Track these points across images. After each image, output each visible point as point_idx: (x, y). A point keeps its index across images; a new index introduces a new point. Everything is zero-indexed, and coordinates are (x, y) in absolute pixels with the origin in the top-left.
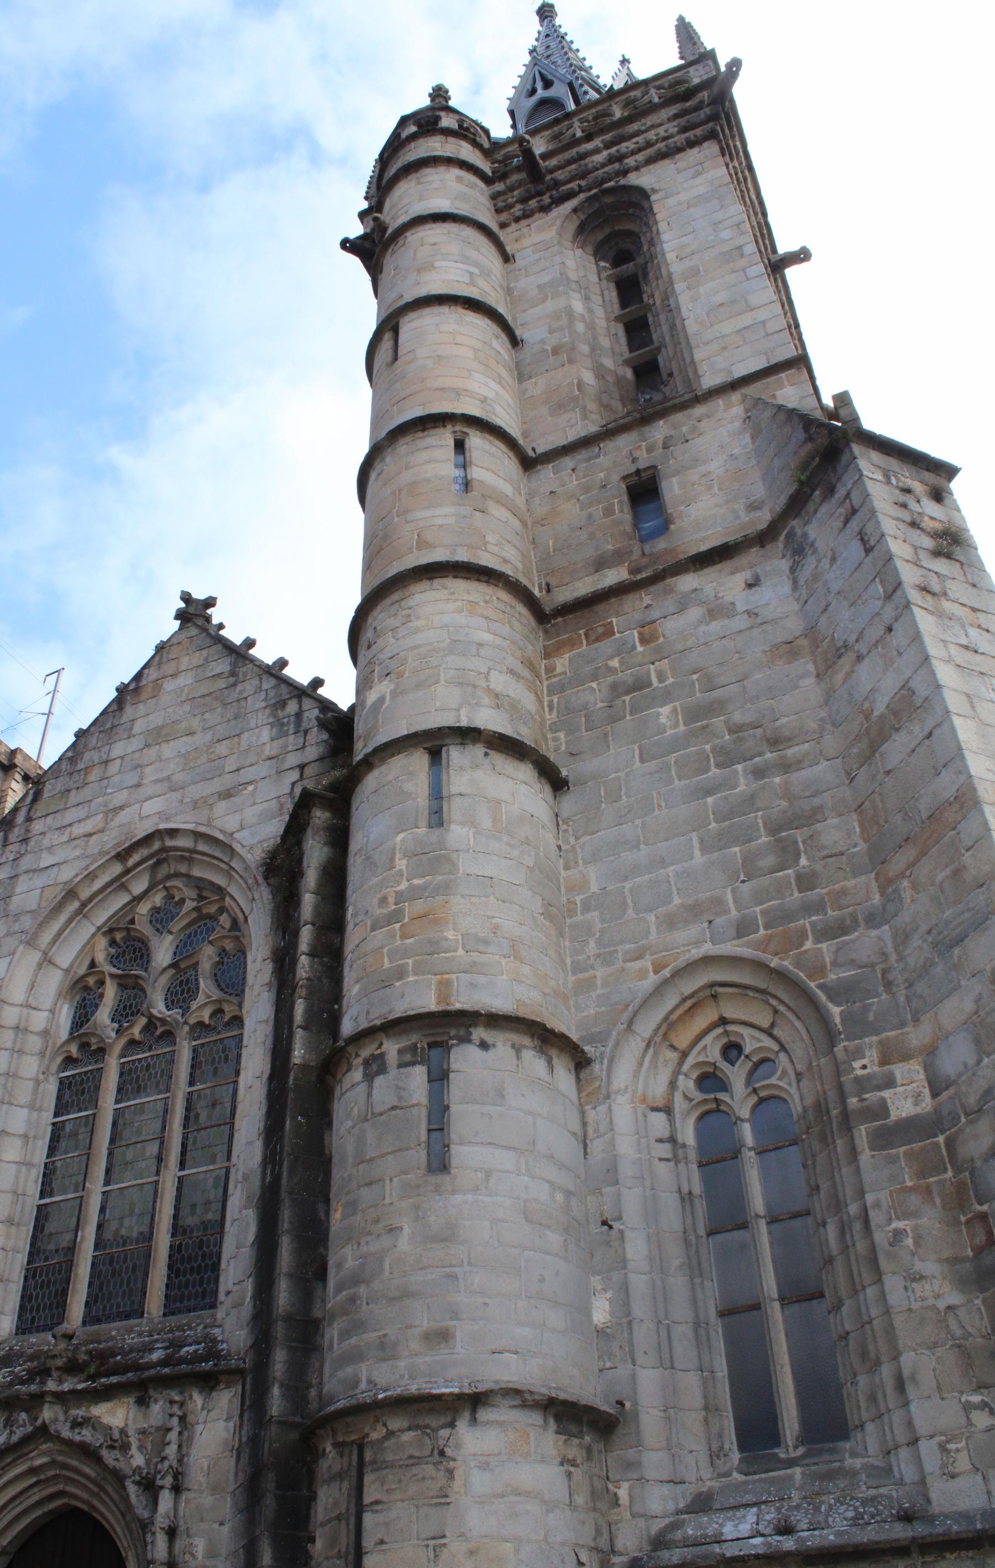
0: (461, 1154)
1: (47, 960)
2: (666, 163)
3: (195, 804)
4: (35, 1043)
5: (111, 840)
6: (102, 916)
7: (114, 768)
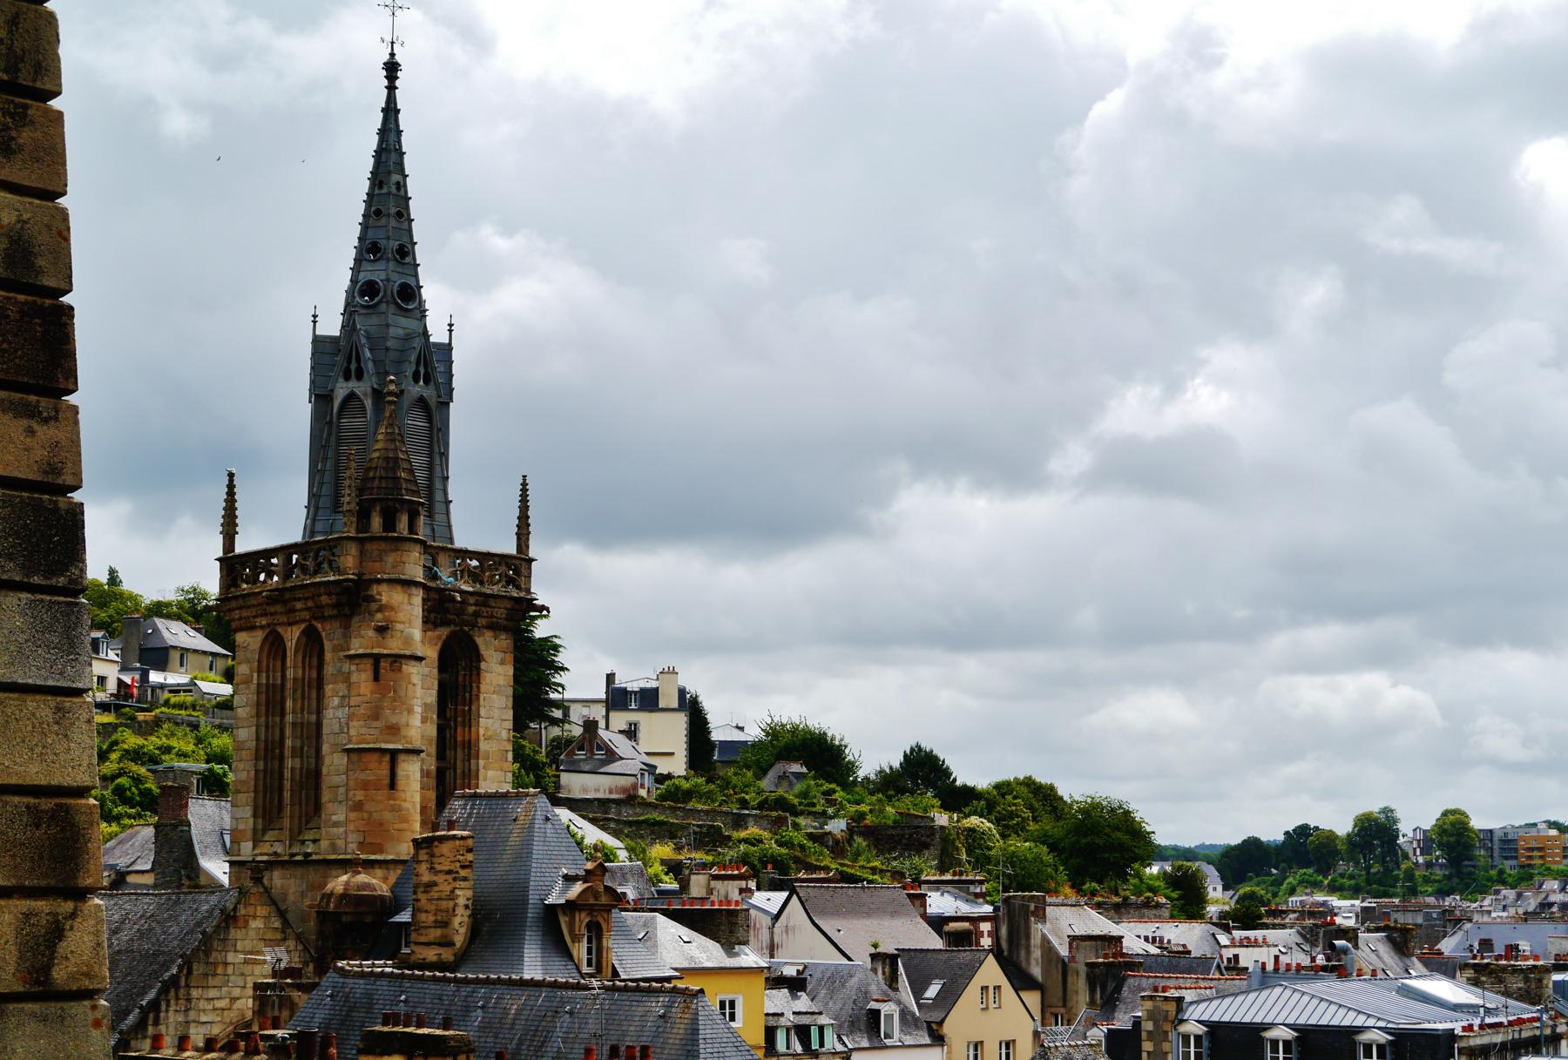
7: (230, 970)
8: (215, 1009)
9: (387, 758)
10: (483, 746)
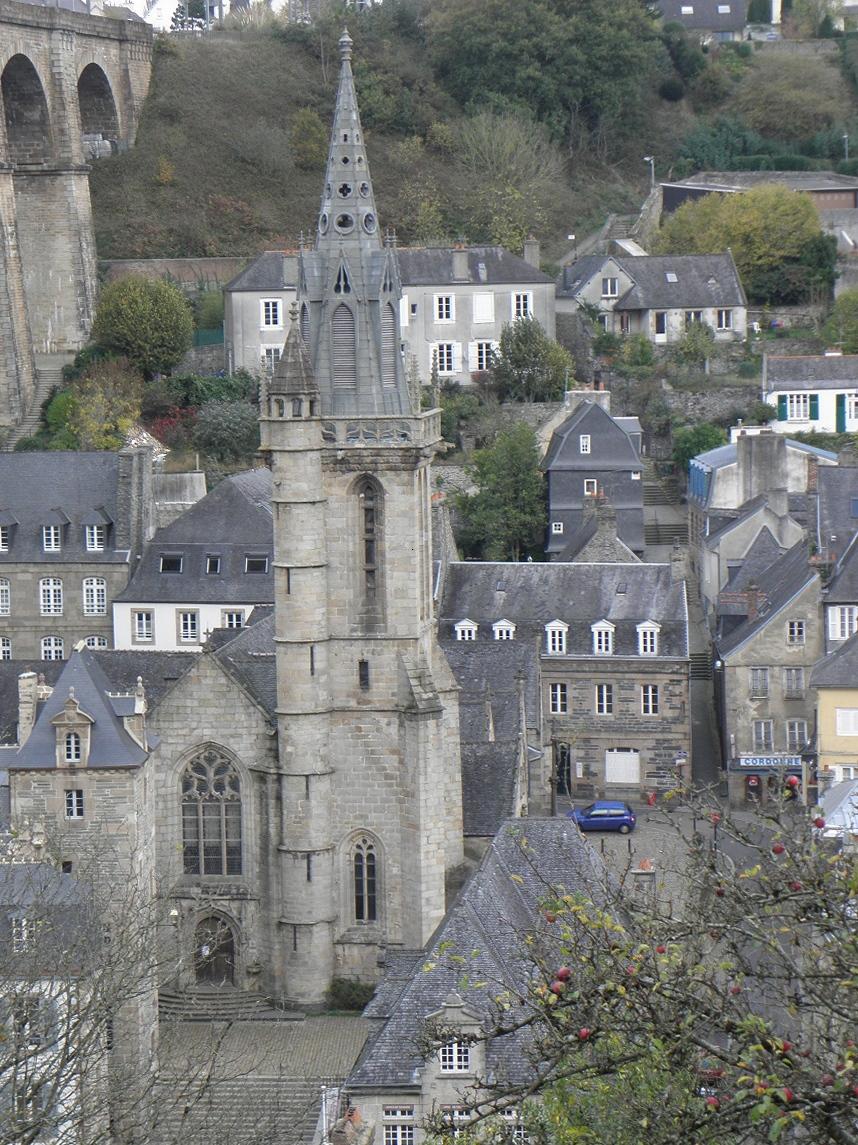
0: (314, 878)
1: (175, 772)
2: (393, 473)
3: (223, 736)
4: (175, 796)
5: (193, 739)
6: (190, 758)
7: (189, 711)
8: (178, 735)
9: (285, 571)
10: (388, 555)
